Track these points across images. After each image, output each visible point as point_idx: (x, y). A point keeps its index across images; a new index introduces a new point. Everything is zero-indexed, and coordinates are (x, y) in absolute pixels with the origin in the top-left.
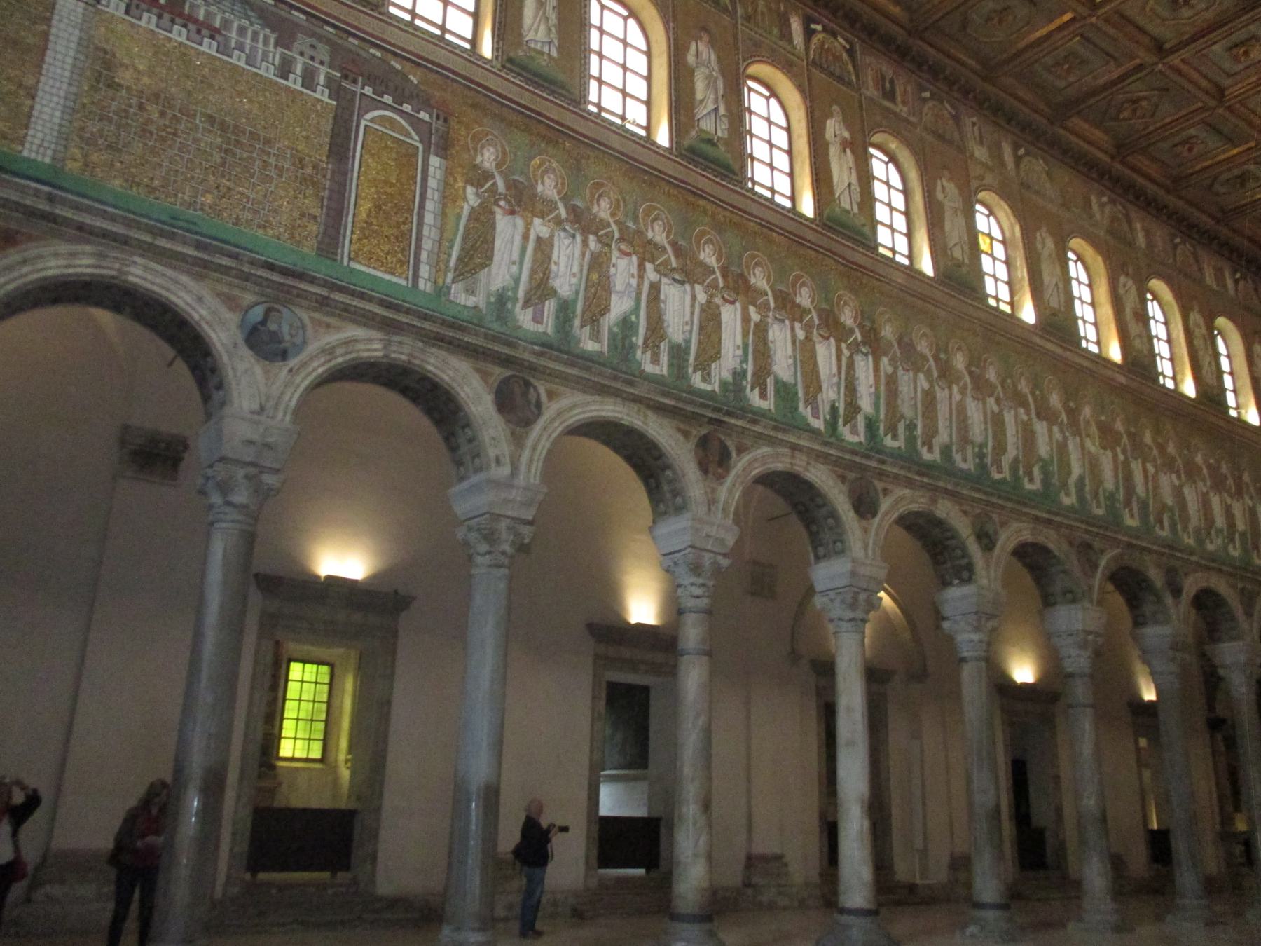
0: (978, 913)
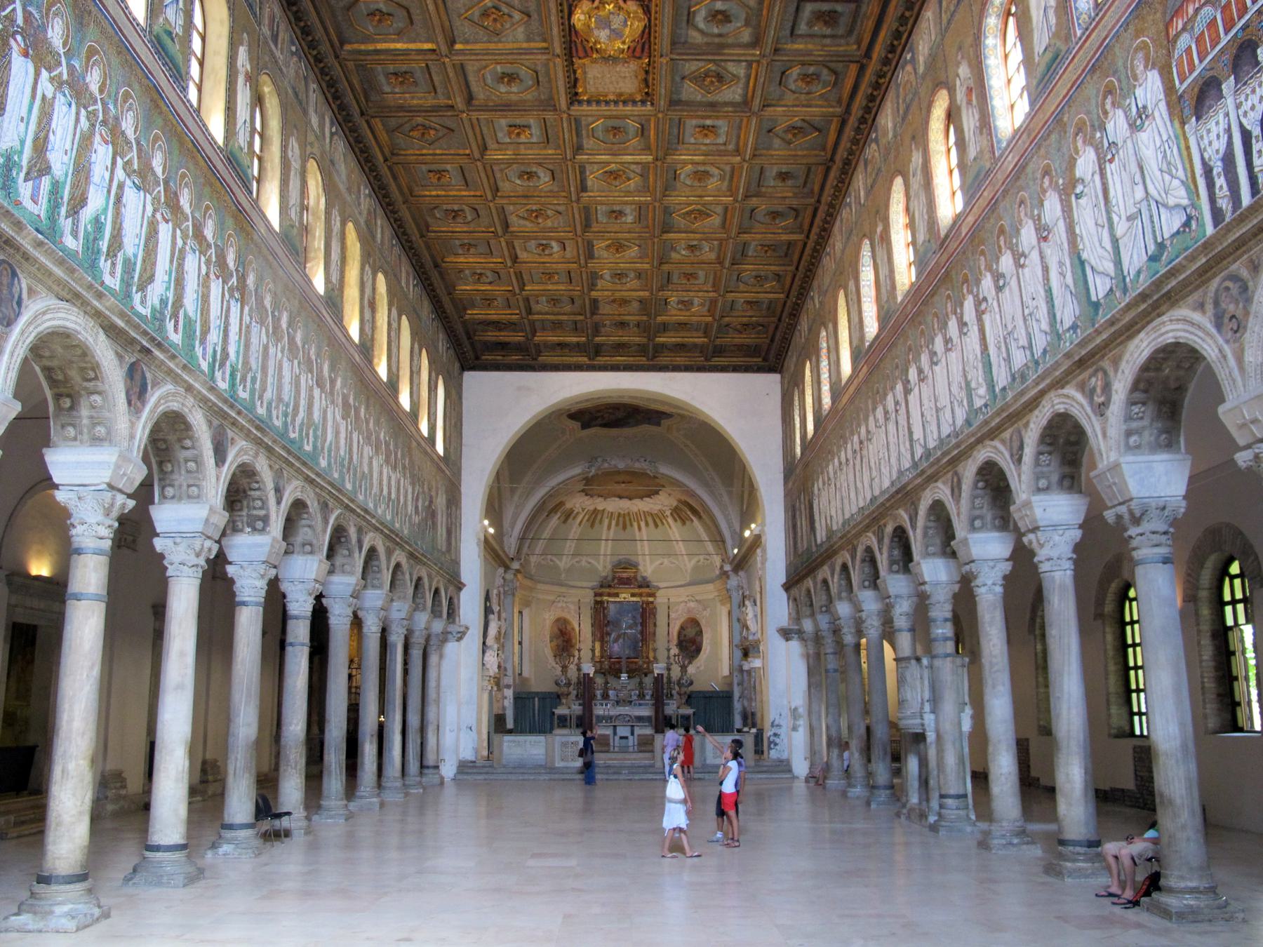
0: (228, 834)
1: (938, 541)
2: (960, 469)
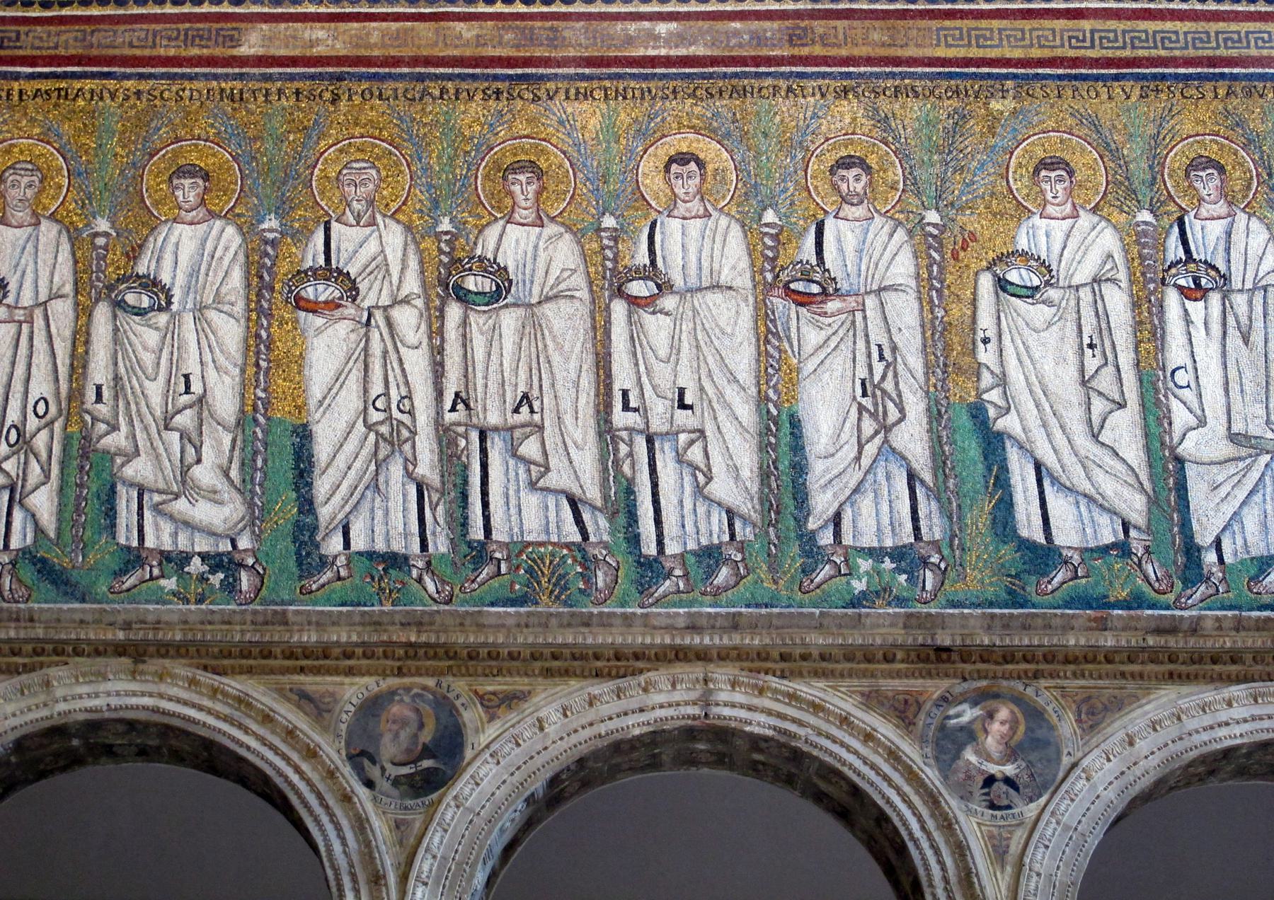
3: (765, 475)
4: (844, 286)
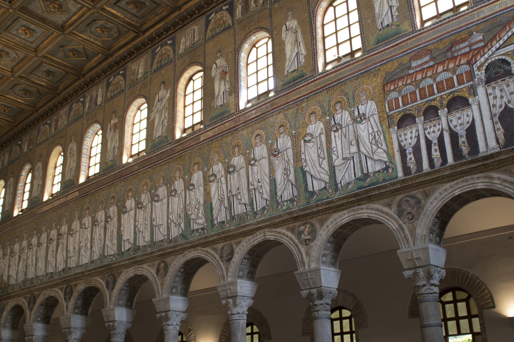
1: (125, 298)
2: (168, 260)
3: (271, 191)
4: (281, 151)
